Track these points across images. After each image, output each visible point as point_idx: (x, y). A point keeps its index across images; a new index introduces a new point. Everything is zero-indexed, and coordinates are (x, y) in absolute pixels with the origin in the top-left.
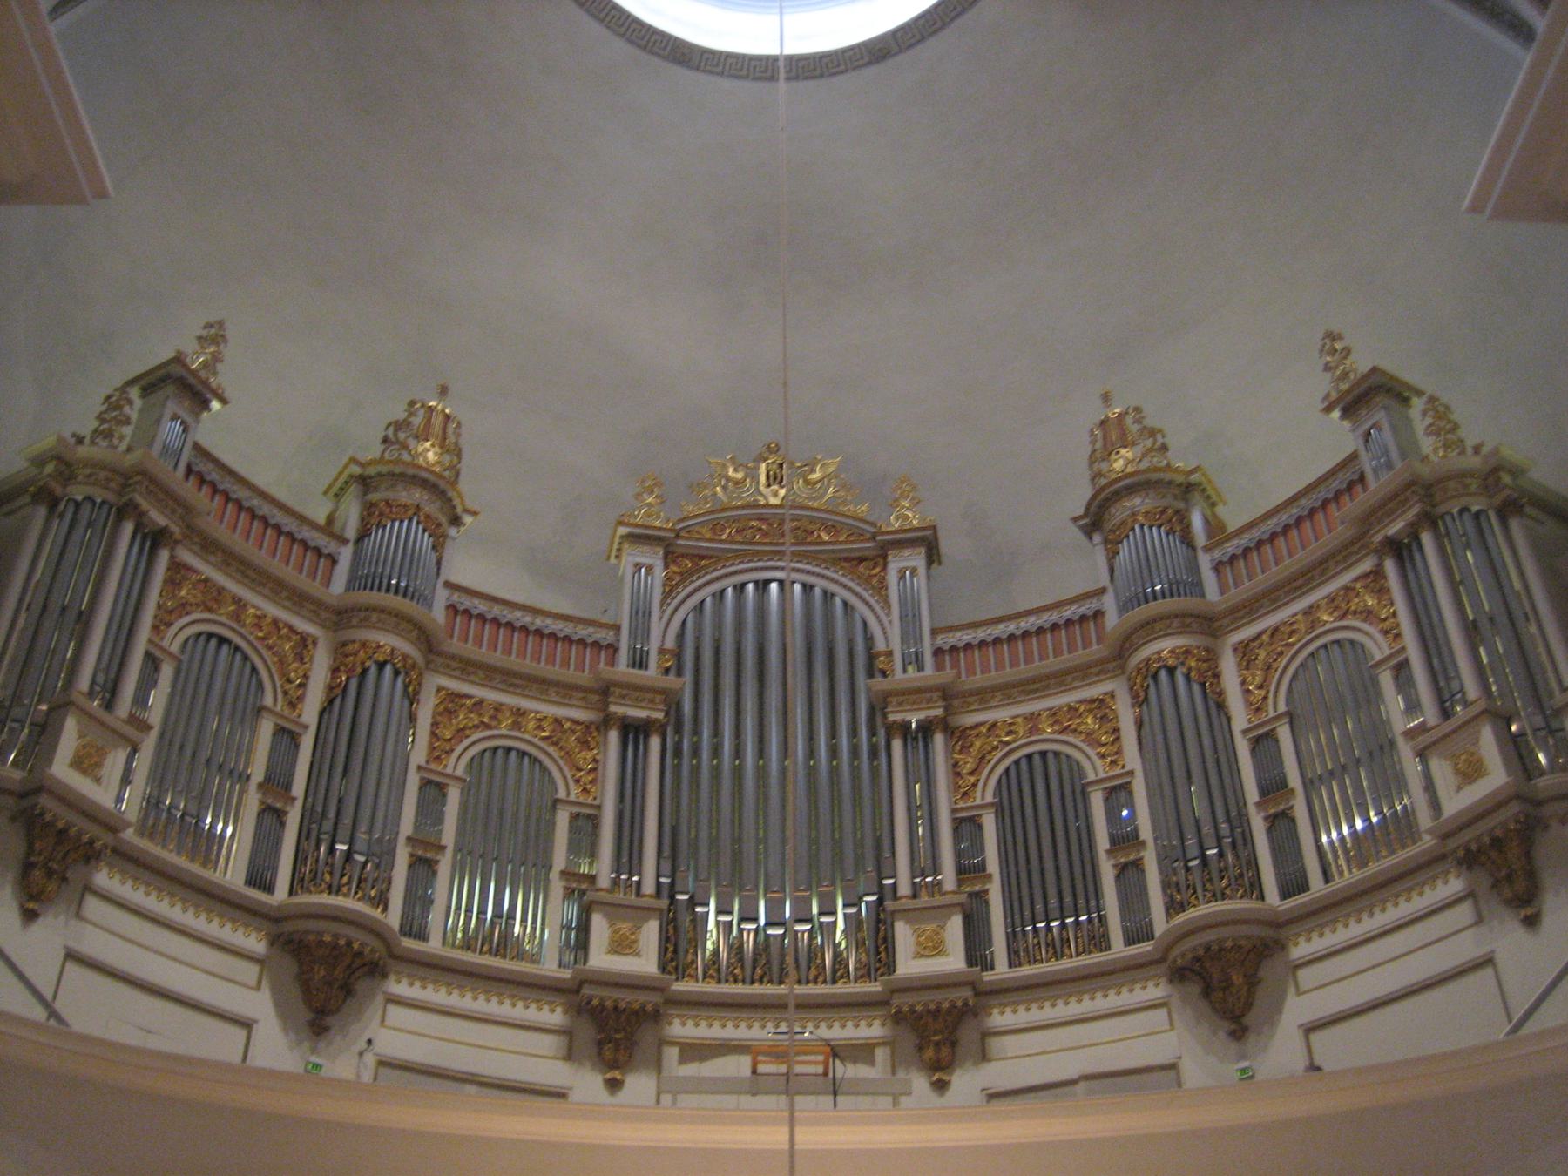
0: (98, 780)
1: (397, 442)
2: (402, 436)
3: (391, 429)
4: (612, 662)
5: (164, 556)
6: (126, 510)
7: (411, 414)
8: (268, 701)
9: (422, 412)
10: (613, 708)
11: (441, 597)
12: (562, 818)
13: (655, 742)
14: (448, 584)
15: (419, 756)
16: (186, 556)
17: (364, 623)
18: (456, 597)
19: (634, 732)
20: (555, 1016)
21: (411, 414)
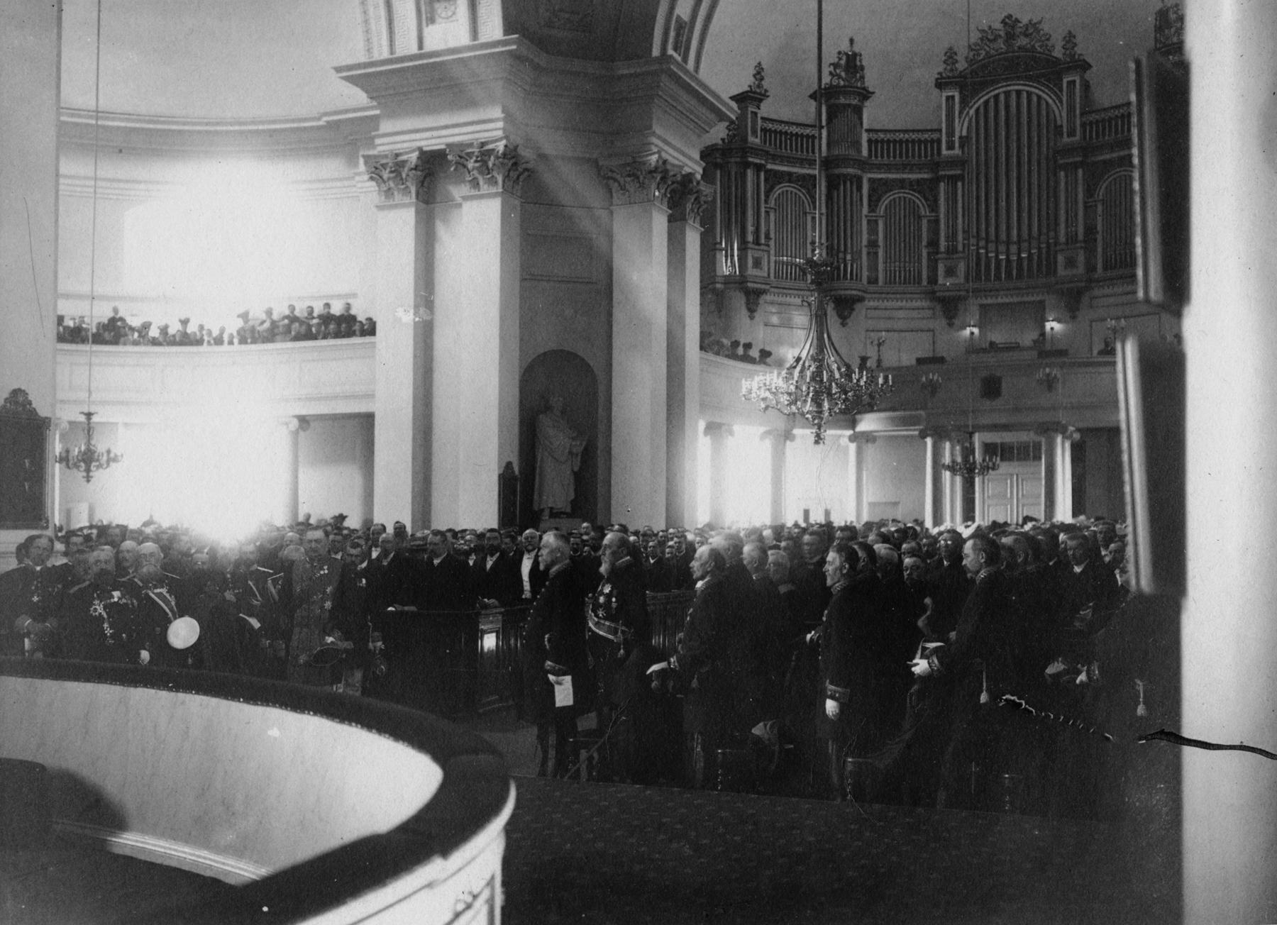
0: (761, 269)
1: (837, 75)
2: (838, 71)
3: (832, 67)
4: (939, 149)
5: (762, 175)
6: (747, 165)
7: (840, 59)
8: (808, 211)
9: (844, 58)
10: (941, 173)
11: (865, 137)
12: (925, 222)
13: (960, 184)
14: (868, 131)
15: (865, 210)
16: (769, 166)
17: (838, 166)
18: (871, 135)
19: (953, 180)
20: (925, 304)
21: (840, 59)
